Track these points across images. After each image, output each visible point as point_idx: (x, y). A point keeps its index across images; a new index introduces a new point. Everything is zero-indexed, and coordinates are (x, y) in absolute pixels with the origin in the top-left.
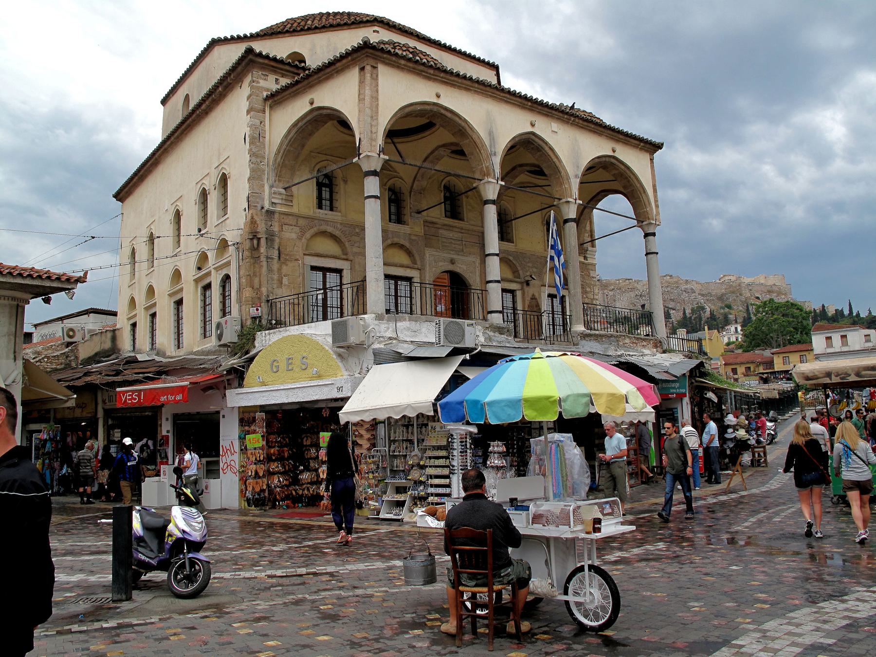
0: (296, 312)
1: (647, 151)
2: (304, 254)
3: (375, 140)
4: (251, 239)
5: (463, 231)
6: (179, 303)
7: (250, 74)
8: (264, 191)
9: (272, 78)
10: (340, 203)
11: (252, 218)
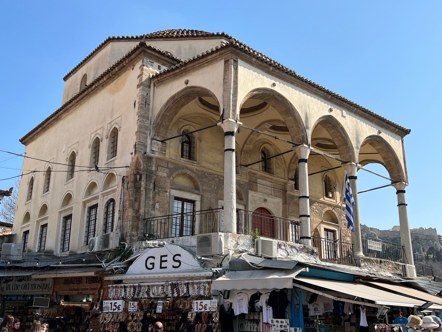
0: (163, 229)
1: (399, 135)
2: (171, 188)
3: (234, 111)
4: (135, 174)
5: (272, 181)
6: (69, 217)
7: (141, 61)
8: (147, 141)
9: (156, 64)
10: (198, 156)
11: (138, 159)
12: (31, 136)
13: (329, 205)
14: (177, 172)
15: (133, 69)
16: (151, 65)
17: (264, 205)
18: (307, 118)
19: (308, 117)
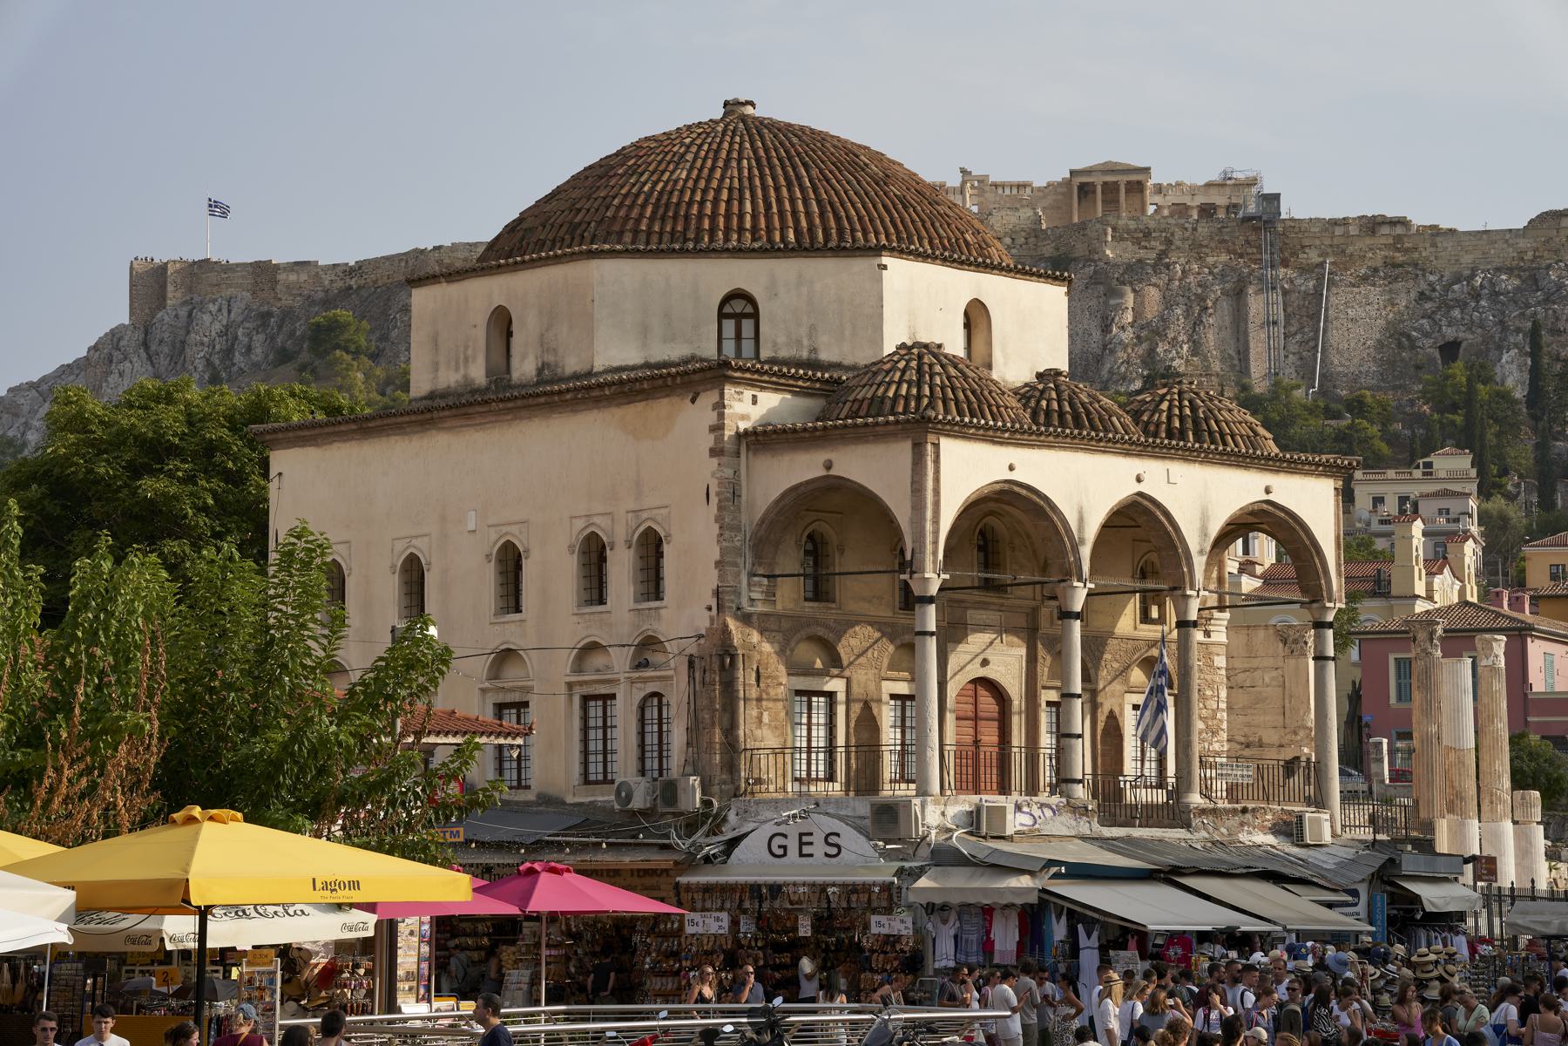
0: (780, 765)
1: (1331, 477)
3: (935, 553)
8: (740, 583)
9: (748, 393)
12: (306, 433)
14: (798, 636)
15: (693, 401)
17: (982, 672)
18: (1081, 520)
19: (1085, 515)
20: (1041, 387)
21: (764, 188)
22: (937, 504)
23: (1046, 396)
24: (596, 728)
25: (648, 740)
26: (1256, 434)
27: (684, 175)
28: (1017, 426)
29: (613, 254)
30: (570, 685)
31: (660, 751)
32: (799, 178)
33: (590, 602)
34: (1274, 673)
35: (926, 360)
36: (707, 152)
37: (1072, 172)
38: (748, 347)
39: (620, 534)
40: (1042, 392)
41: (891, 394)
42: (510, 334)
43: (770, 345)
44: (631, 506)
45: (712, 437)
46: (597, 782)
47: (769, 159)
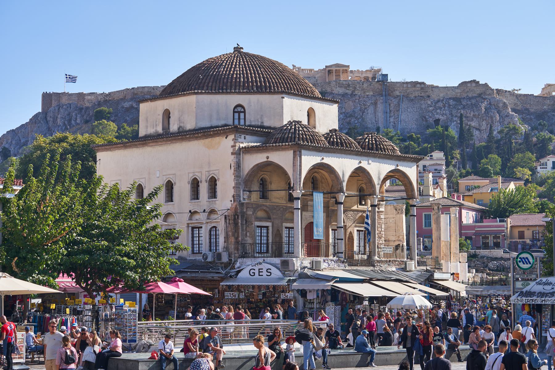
0: (252, 248)
1: (415, 162)
3: (300, 185)
9: (243, 136)
11: (236, 206)
12: (108, 147)
13: (361, 211)
14: (258, 209)
15: (226, 138)
16: (241, 138)
18: (343, 174)
20: (331, 134)
21: (247, 73)
22: (300, 170)
23: (333, 137)
24: (196, 237)
25: (212, 241)
26: (394, 149)
27: (222, 70)
28: (325, 146)
29: (201, 93)
30: (188, 224)
31: (216, 244)
32: (257, 71)
33: (194, 199)
34: (393, 219)
35: (297, 126)
36: (229, 63)
37: (326, 66)
38: (242, 122)
39: (204, 179)
40: (331, 136)
41: (286, 136)
42: (169, 117)
43: (249, 121)
44: (207, 170)
45: (232, 149)
46: (196, 253)
47: (248, 65)
